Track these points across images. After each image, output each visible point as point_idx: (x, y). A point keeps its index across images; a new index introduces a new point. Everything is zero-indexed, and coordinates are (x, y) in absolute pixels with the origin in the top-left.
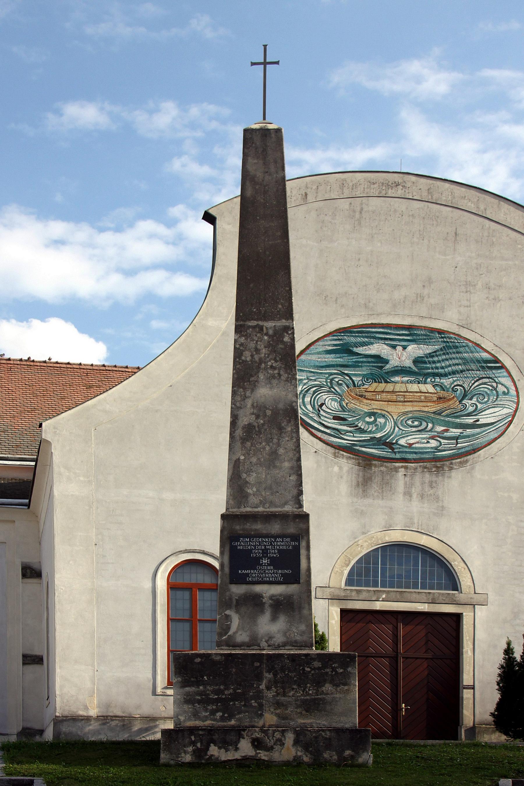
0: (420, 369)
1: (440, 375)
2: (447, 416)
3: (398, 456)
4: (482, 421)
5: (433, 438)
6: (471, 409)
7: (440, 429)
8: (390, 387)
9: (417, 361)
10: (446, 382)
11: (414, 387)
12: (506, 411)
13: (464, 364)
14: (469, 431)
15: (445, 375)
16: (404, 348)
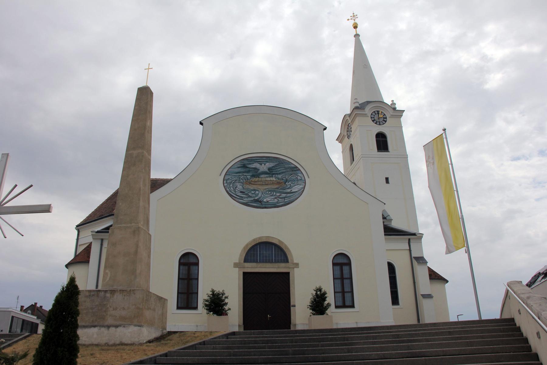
0: (270, 172)
1: (277, 174)
2: (281, 189)
3: (264, 206)
4: (293, 191)
5: (276, 198)
6: (289, 186)
7: (278, 194)
8: (260, 179)
9: (269, 169)
10: (280, 176)
11: (269, 179)
12: (301, 186)
13: (286, 169)
14: (289, 195)
15: (280, 174)
16: (265, 164)
